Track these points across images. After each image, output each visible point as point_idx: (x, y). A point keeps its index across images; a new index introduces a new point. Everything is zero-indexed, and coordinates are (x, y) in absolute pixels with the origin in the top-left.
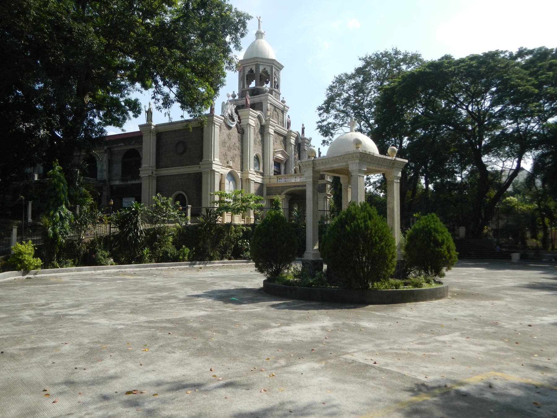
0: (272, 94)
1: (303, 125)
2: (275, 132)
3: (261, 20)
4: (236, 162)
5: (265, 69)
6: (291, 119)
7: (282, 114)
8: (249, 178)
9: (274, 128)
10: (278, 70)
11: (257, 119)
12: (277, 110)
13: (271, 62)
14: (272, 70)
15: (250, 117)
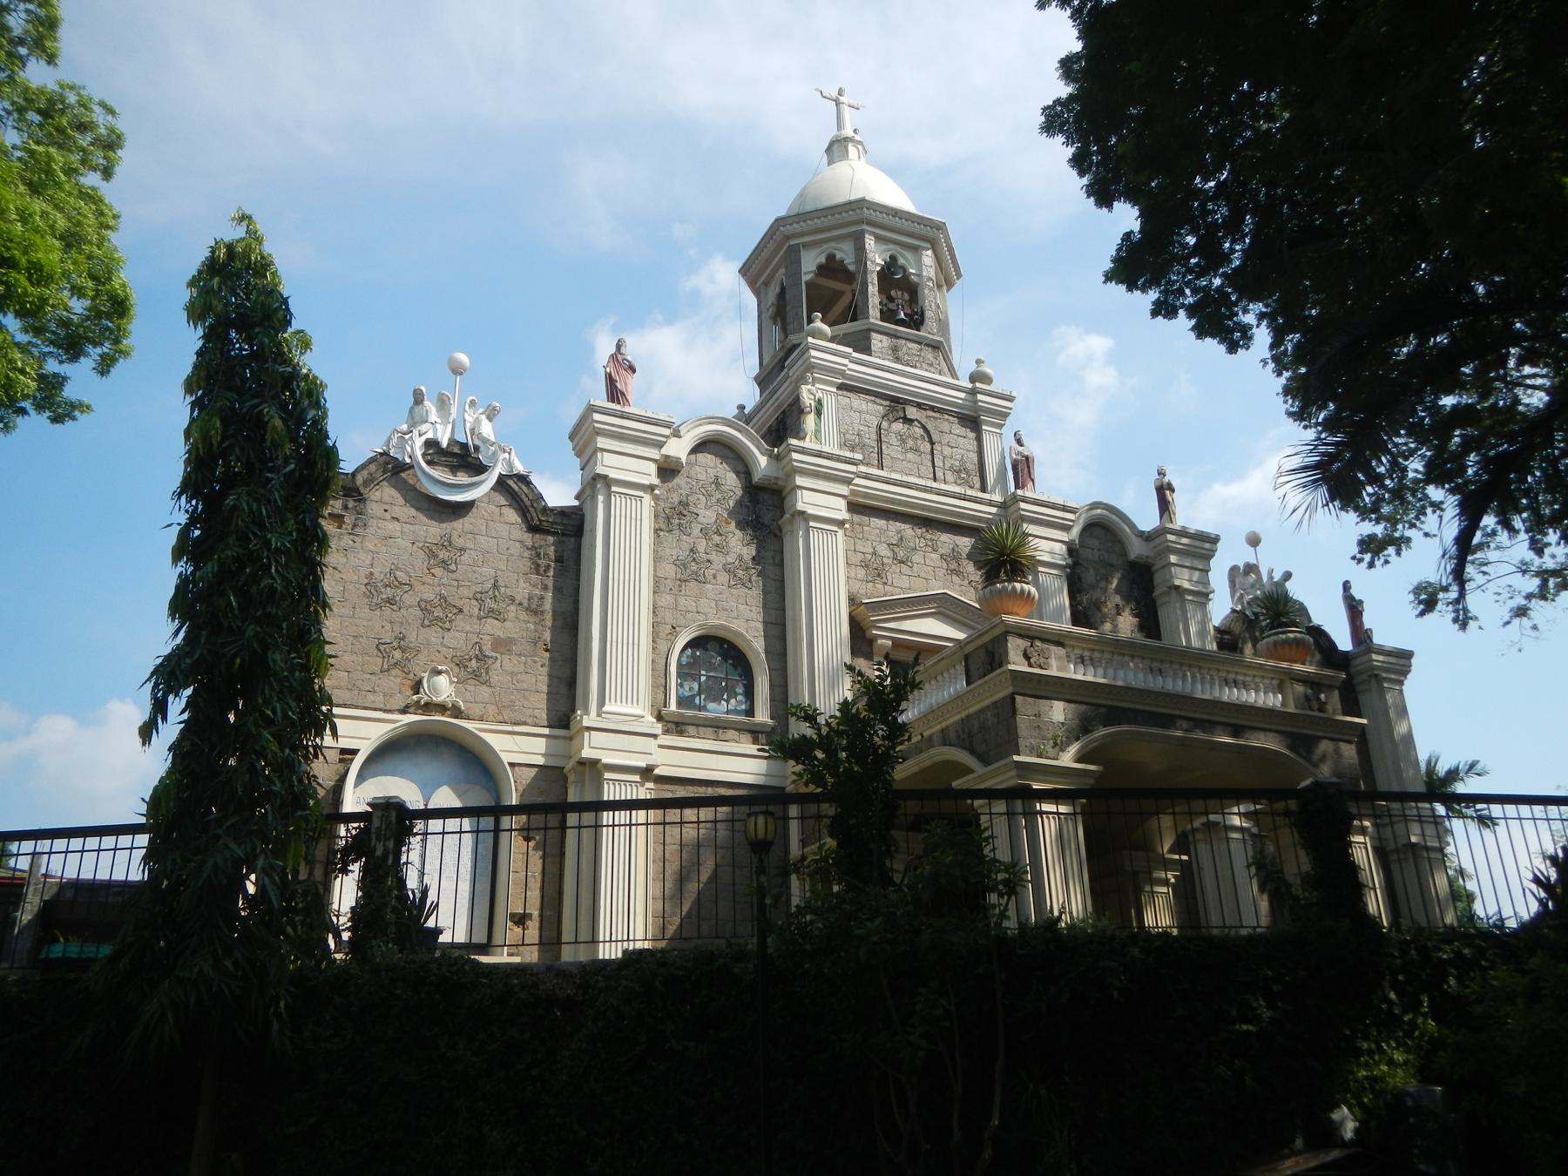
0: (867, 350)
1: (1161, 473)
2: (853, 507)
3: (842, 99)
4: (495, 677)
5: (831, 257)
6: (1032, 448)
7: (958, 430)
8: (587, 753)
9: (844, 490)
10: (916, 250)
11: (706, 459)
12: (912, 412)
13: (852, 216)
14: (860, 249)
15: (602, 442)
